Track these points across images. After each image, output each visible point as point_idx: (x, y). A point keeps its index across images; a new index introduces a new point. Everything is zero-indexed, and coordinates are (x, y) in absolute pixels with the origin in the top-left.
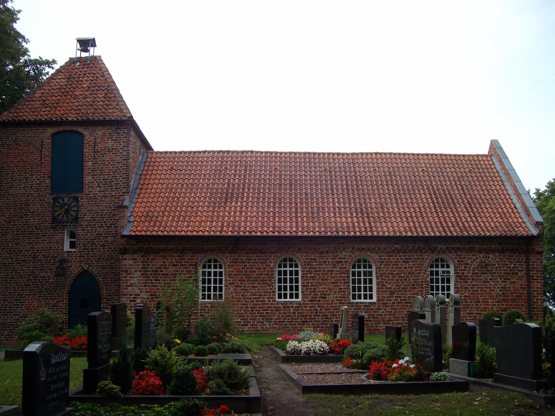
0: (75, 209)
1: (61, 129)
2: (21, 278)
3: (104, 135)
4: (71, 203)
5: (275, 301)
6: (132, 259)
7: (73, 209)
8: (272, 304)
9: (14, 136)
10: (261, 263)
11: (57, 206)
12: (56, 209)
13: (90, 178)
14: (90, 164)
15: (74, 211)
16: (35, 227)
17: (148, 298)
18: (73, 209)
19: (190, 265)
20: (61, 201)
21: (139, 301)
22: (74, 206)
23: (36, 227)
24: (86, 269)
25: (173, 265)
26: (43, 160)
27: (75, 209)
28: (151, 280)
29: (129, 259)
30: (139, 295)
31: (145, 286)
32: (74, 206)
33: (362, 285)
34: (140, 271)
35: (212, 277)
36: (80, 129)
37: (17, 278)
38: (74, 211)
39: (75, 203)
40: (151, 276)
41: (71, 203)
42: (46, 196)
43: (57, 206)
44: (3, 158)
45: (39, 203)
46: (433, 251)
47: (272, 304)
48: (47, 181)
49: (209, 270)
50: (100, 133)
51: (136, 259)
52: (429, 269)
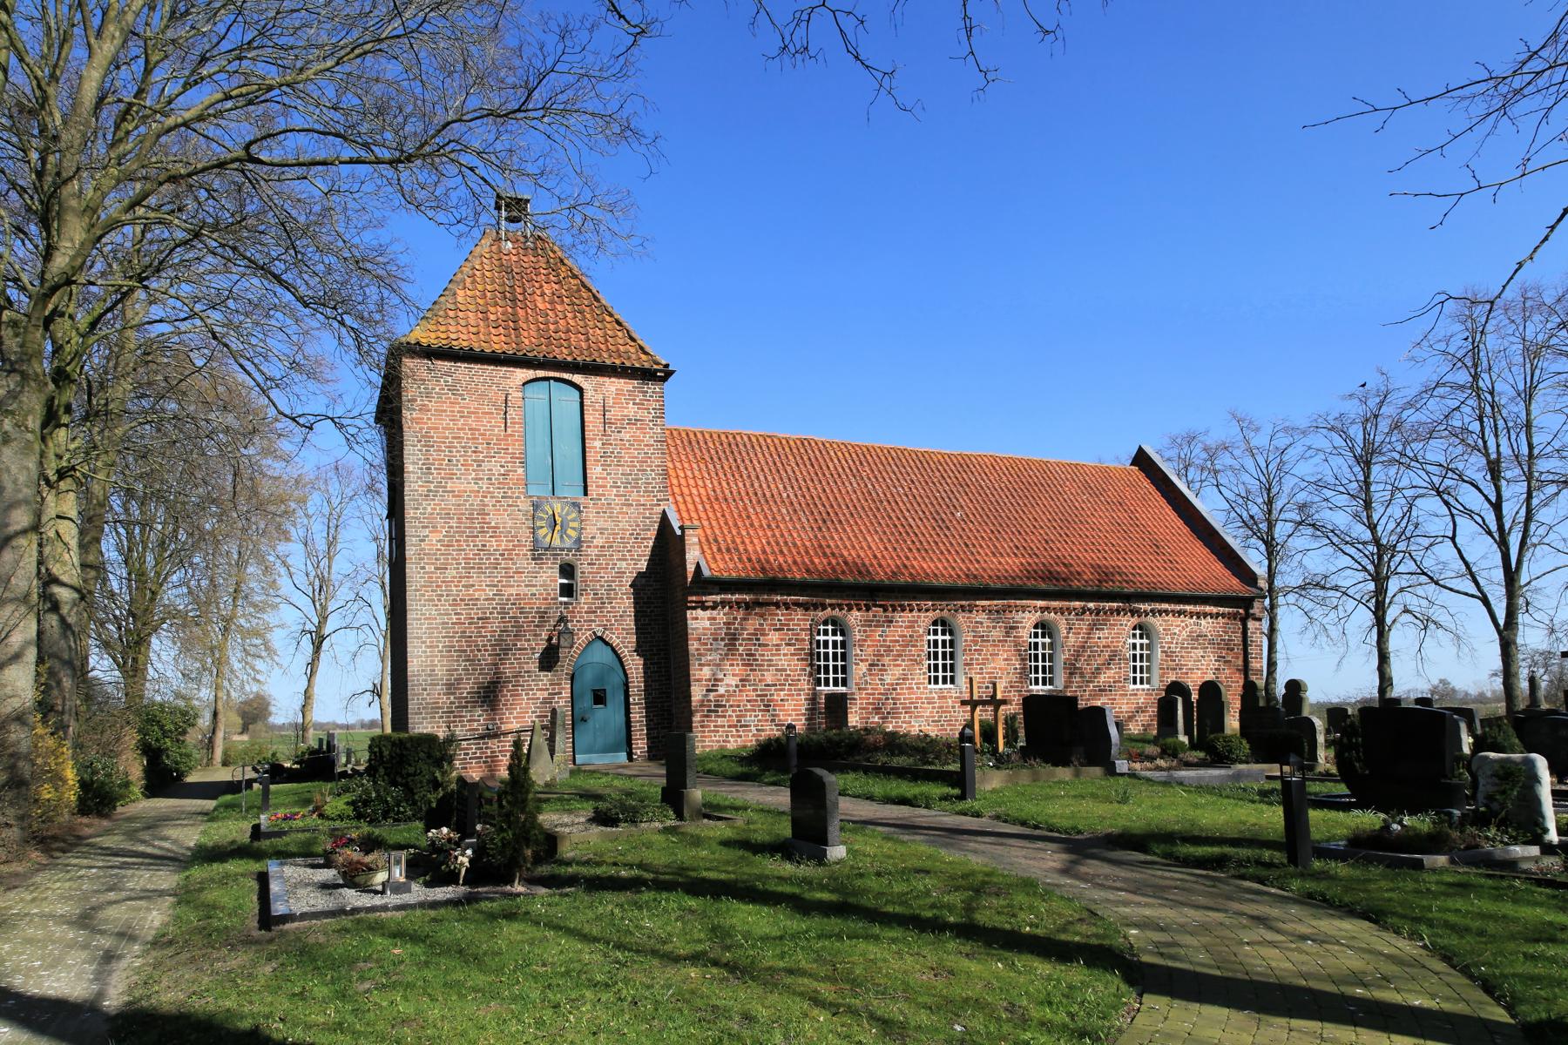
0: (575, 525)
1: (541, 373)
2: (479, 650)
3: (619, 393)
4: (567, 514)
5: (925, 688)
6: (709, 619)
7: (572, 524)
8: (922, 693)
9: (450, 379)
10: (907, 627)
11: (542, 519)
12: (539, 524)
13: (599, 469)
14: (598, 444)
15: (574, 529)
16: (503, 555)
17: (737, 686)
18: (572, 524)
19: (802, 630)
20: (547, 508)
21: (721, 690)
22: (573, 520)
23: (503, 555)
24: (599, 634)
25: (775, 630)
26: (509, 430)
27: (575, 525)
28: (741, 655)
29: (703, 619)
30: (721, 680)
31: (732, 665)
32: (573, 520)
33: (1040, 664)
34: (722, 639)
35: (830, 650)
36: (577, 378)
37: (472, 651)
38: (574, 529)
39: (574, 515)
40: (741, 648)
41: (567, 514)
42: (518, 497)
43: (542, 519)
44: (429, 419)
45: (505, 510)
46: (1133, 612)
47: (922, 693)
48: (520, 471)
49: (826, 638)
50: (613, 389)
51: (714, 619)
52: (1131, 641)
